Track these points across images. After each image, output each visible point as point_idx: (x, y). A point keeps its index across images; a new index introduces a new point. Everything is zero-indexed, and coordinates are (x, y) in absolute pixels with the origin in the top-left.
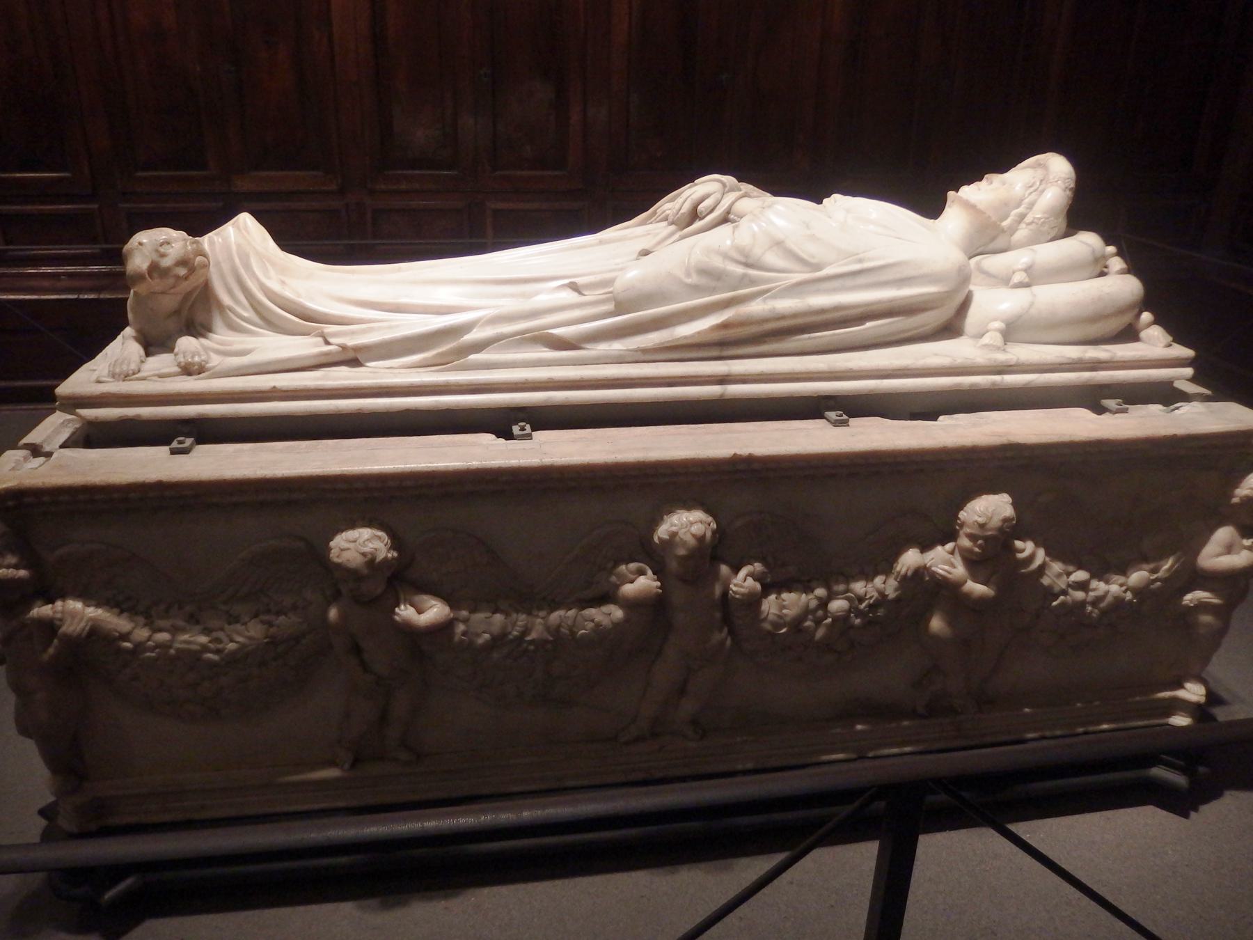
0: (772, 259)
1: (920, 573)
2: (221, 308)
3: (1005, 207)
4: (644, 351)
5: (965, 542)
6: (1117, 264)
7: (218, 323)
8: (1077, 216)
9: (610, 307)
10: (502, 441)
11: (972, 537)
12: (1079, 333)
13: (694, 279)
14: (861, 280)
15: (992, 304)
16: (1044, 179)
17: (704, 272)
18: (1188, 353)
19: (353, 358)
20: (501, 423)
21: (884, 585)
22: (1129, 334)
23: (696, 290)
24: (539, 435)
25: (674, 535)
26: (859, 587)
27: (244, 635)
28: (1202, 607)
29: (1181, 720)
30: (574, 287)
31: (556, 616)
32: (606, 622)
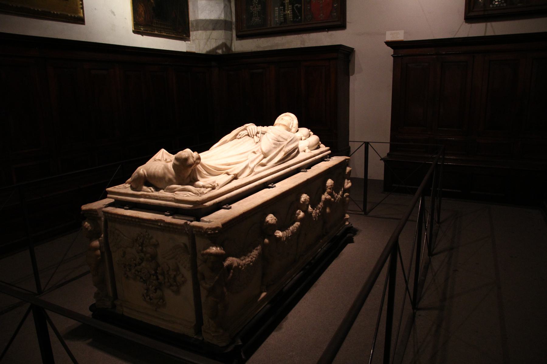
0: (281, 140)
1: (326, 199)
2: (200, 172)
3: (289, 124)
4: (276, 163)
5: (329, 190)
6: (312, 133)
7: (199, 178)
8: (300, 125)
9: (262, 156)
10: (271, 189)
11: (330, 189)
12: (314, 148)
13: (274, 146)
14: (292, 141)
15: (303, 145)
16: (288, 119)
17: (274, 144)
18: (328, 148)
19: (236, 178)
20: (265, 186)
21: (321, 204)
22: (318, 147)
23: (275, 148)
24: (277, 185)
25: (305, 200)
26: (319, 206)
27: (255, 253)
28: (347, 196)
29: (347, 223)
30: (254, 152)
31: (291, 228)
32: (297, 226)
